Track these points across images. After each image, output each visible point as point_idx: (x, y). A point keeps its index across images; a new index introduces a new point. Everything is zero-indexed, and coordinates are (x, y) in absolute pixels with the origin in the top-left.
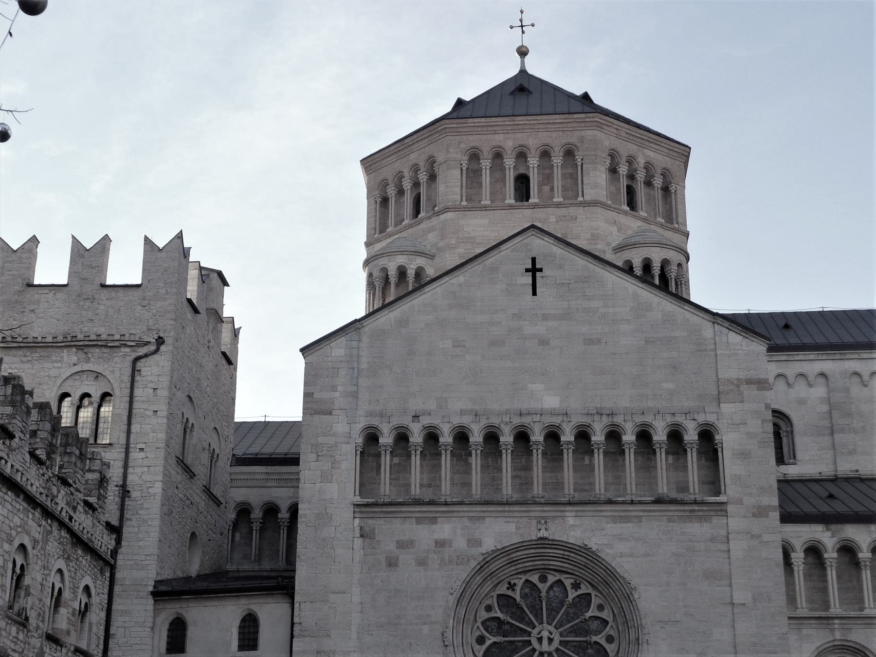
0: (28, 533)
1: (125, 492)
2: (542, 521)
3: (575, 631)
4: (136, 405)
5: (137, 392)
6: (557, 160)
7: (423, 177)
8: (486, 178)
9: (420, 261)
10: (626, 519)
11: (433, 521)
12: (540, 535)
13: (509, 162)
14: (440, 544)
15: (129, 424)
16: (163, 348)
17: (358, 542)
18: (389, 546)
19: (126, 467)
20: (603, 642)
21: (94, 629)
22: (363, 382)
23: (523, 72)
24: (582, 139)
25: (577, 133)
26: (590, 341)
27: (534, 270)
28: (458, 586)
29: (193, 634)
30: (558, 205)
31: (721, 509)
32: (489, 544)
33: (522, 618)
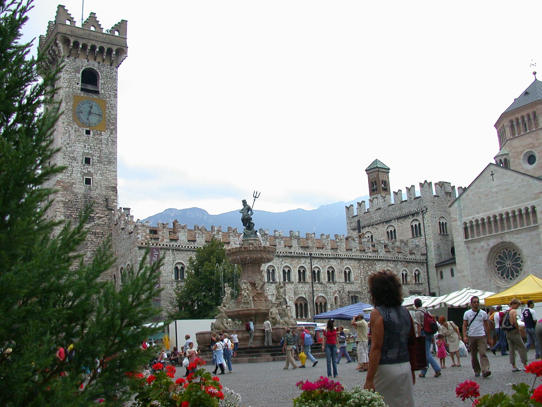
0: (390, 267)
1: (426, 245)
2: (502, 238)
3: (515, 261)
4: (425, 225)
5: (425, 222)
6: (532, 117)
7: (503, 131)
8: (516, 127)
9: (505, 157)
10: (518, 234)
11: (480, 242)
12: (502, 240)
13: (520, 121)
14: (482, 247)
15: (424, 230)
16: (428, 210)
17: (466, 249)
18: (472, 250)
19: (425, 240)
20: (521, 263)
21: (422, 277)
22: (463, 212)
23: (536, 80)
24: (537, 109)
25: (536, 108)
26: (507, 190)
27: (492, 175)
28: (486, 256)
29: (444, 274)
30: (534, 131)
31: (537, 227)
32: (492, 245)
33: (504, 260)
